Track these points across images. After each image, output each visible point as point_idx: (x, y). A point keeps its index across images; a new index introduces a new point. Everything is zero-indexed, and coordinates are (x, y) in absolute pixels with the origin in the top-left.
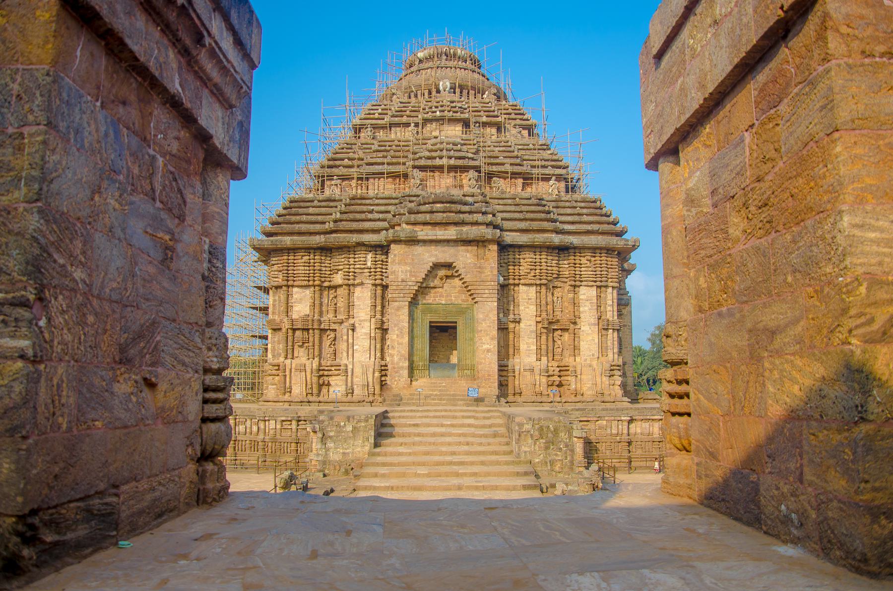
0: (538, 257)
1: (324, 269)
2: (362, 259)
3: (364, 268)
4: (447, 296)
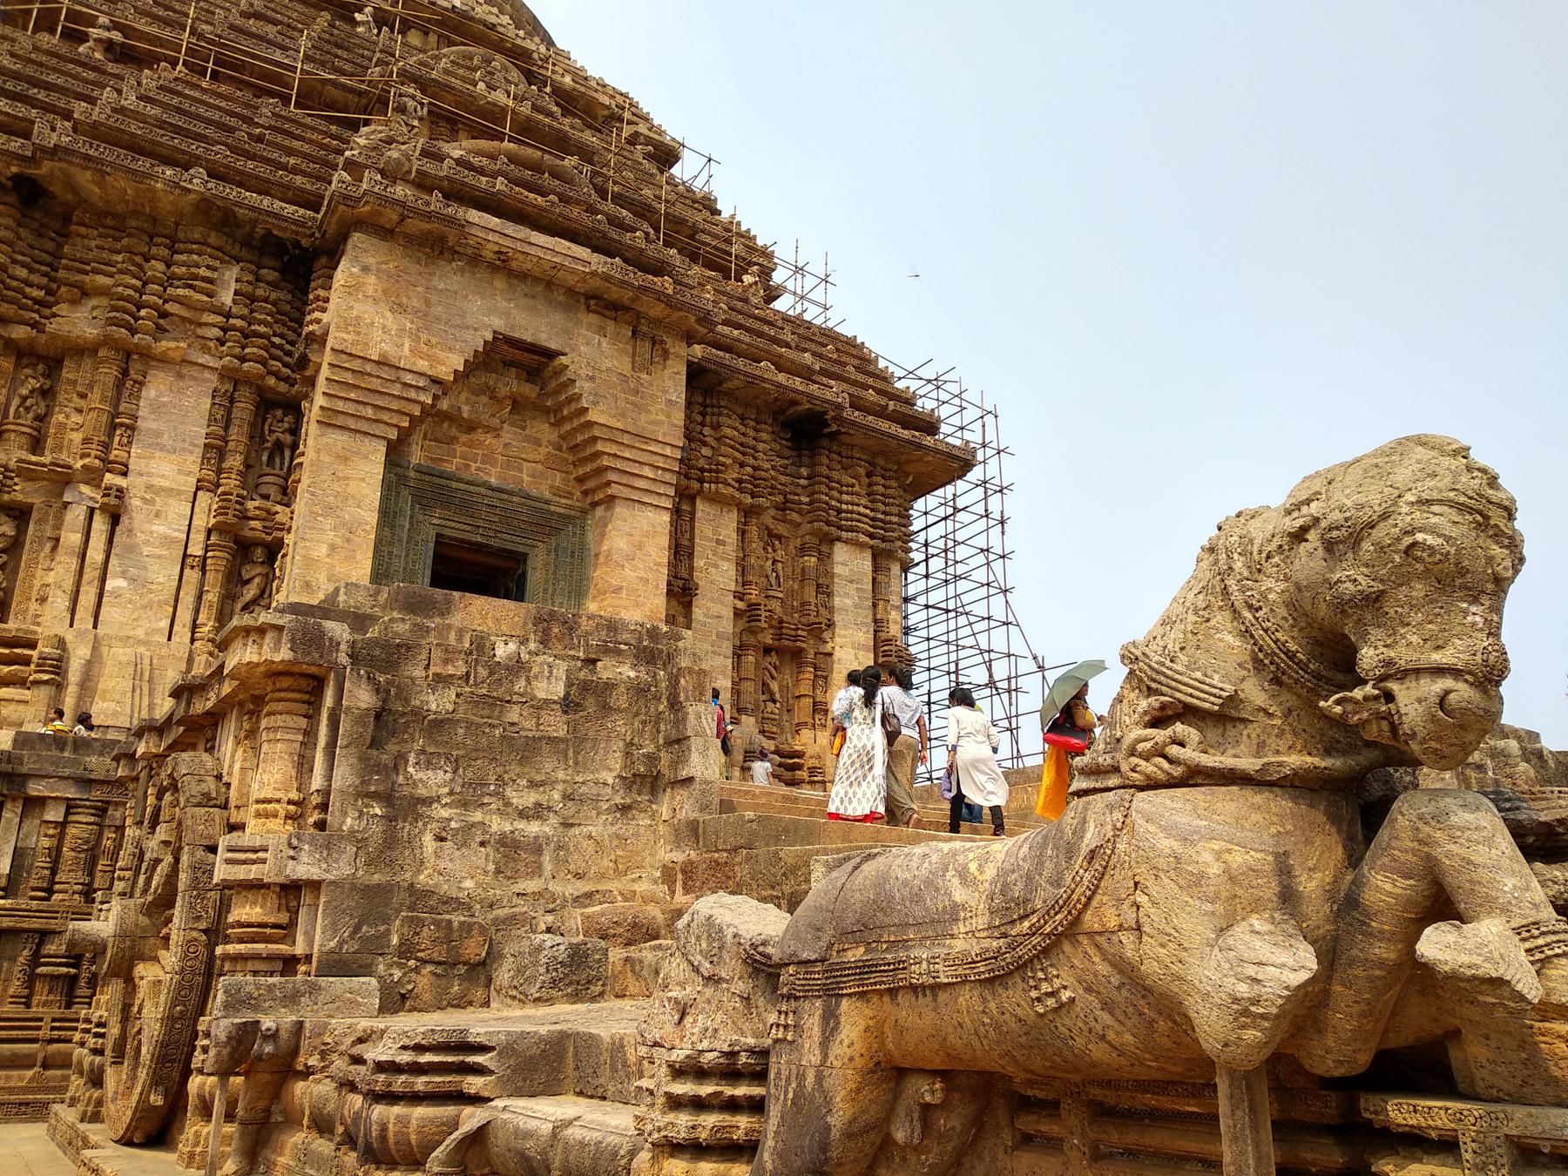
0: (751, 433)
1: (22, 273)
2: (203, 272)
3: (203, 309)
4: (506, 466)
